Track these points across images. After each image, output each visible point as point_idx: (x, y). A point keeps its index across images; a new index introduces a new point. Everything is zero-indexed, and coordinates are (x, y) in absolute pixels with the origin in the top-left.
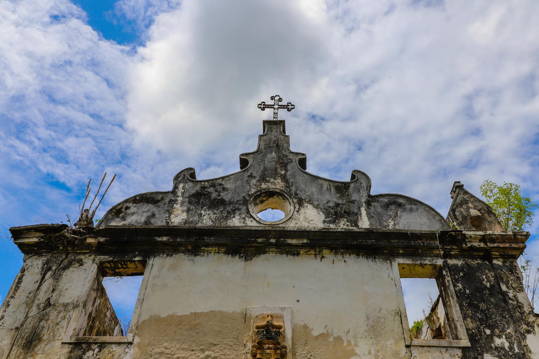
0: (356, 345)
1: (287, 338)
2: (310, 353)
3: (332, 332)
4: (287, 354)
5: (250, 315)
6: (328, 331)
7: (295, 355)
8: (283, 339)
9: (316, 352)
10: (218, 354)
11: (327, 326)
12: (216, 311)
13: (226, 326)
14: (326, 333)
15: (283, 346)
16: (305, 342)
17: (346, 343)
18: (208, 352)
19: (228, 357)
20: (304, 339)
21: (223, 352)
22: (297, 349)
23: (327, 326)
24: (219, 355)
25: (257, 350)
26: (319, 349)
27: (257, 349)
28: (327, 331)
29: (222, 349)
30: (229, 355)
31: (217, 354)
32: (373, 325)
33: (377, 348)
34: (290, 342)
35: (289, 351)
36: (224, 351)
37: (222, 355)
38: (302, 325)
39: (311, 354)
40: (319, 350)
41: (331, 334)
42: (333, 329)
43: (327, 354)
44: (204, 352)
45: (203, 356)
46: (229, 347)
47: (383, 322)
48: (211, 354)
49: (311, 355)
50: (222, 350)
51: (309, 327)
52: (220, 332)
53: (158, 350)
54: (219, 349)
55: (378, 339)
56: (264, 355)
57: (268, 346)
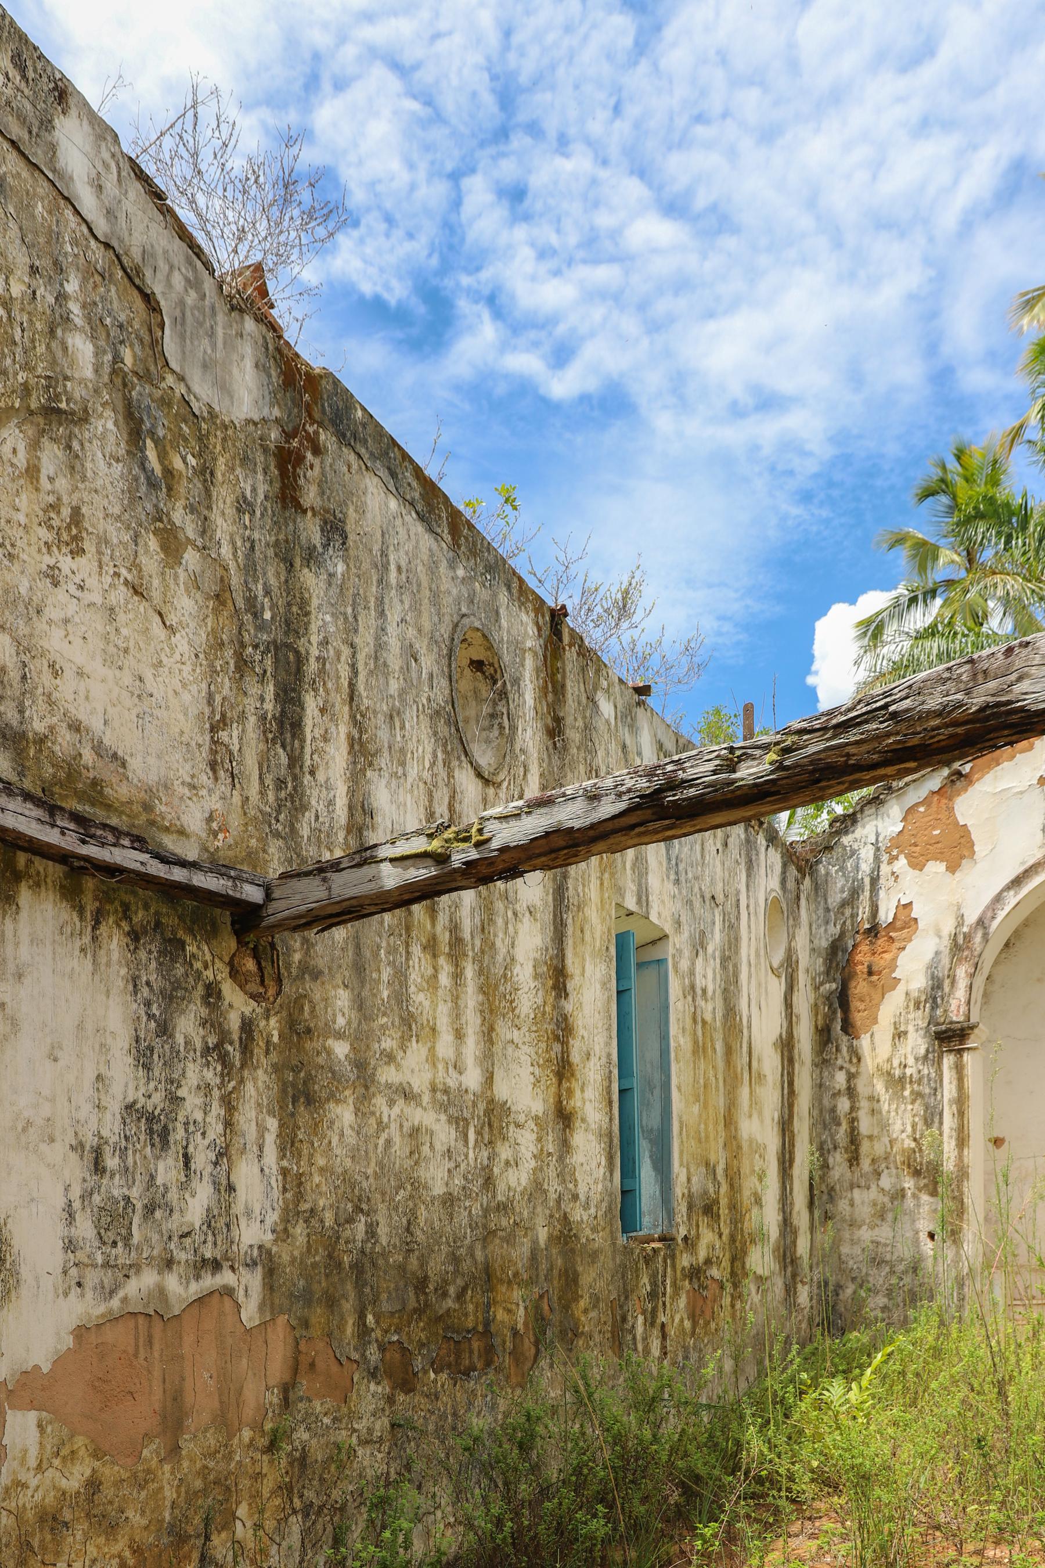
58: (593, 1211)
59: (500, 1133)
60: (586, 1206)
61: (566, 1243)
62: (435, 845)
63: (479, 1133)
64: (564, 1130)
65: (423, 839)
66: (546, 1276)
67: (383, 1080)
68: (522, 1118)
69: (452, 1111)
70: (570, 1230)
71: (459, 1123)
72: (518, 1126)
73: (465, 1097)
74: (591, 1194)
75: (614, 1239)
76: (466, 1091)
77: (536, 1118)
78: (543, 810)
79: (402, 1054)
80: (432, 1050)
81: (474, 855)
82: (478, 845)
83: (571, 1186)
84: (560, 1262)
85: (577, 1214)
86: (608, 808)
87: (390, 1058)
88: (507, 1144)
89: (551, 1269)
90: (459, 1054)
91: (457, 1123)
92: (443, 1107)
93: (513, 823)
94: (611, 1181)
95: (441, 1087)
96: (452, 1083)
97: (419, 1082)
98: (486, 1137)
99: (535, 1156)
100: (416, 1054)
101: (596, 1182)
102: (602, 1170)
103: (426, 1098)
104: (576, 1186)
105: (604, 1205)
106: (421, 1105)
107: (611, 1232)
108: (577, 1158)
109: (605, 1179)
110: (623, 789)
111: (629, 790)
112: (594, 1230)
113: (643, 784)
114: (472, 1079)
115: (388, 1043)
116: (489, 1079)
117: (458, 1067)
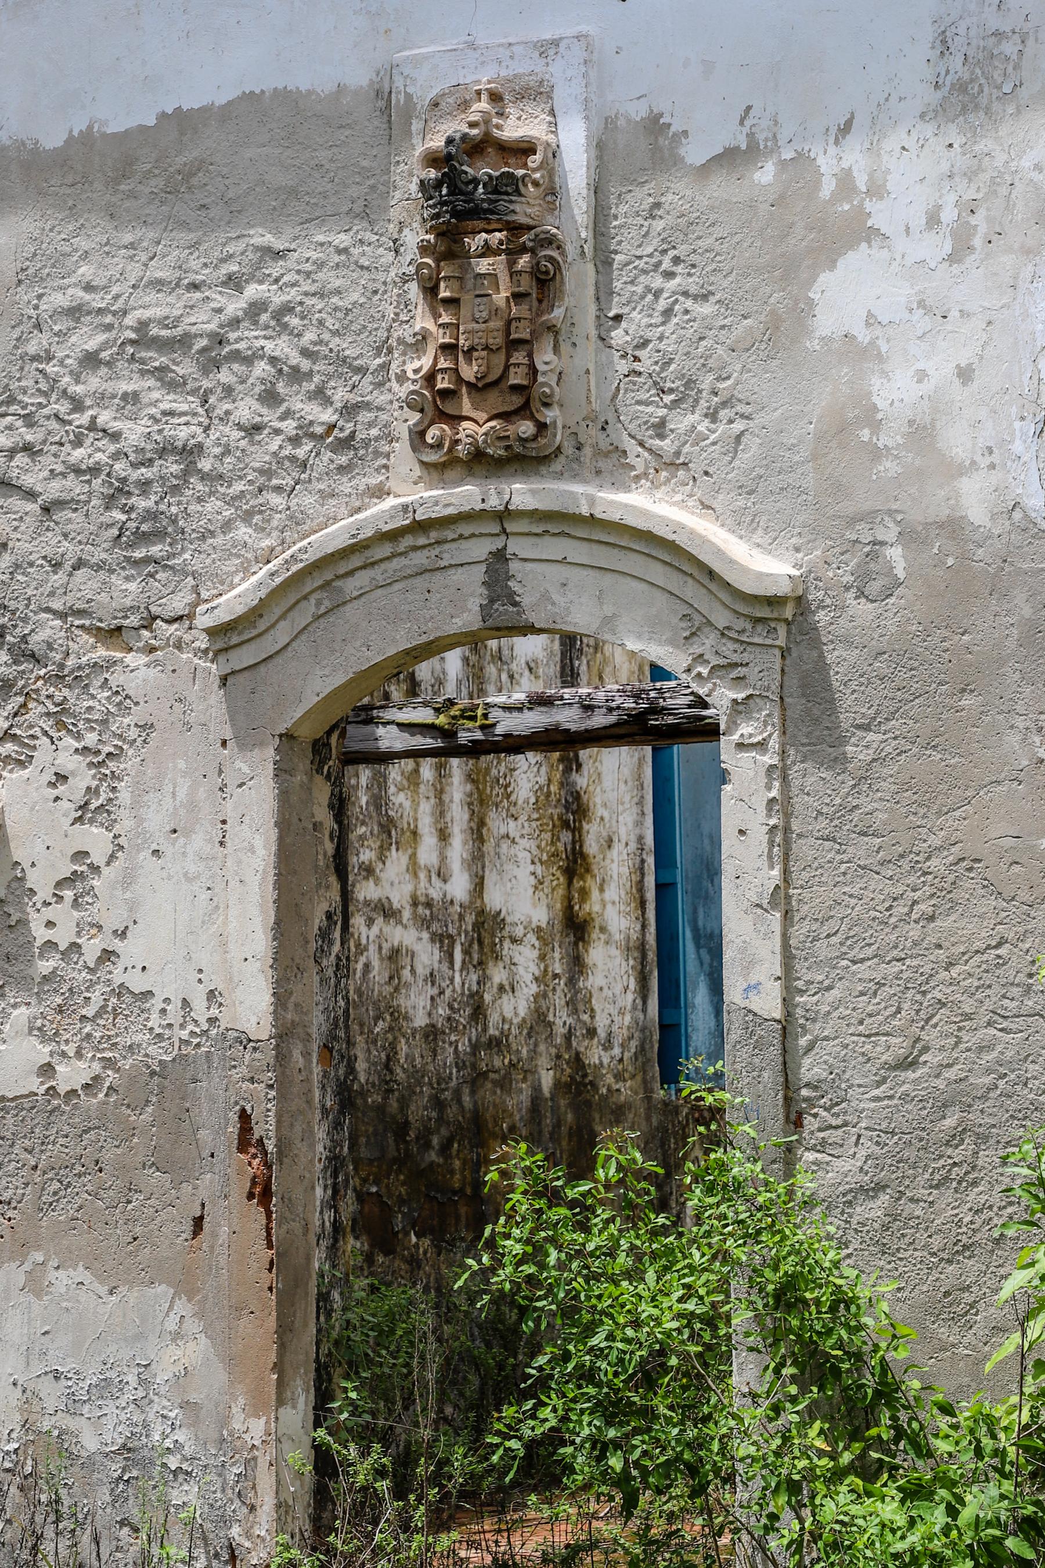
0: (877, 190)
1: (567, 190)
2: (674, 247)
3: (775, 136)
4: (560, 269)
5: (409, 97)
6: (753, 134)
7: (609, 263)
8: (549, 198)
9: (700, 243)
10: (293, 291)
11: (749, 108)
12: (263, 92)
13: (313, 163)
14: (744, 147)
15: (542, 236)
16: (651, 200)
17: (833, 187)
18: (256, 286)
19: (335, 300)
20: (647, 186)
21: (314, 281)
22: (618, 238)
23: (749, 108)
24: (298, 299)
25: (442, 264)
26: (713, 224)
27: (438, 261)
28: (751, 136)
29: (308, 267)
30: (338, 292)
31: (292, 295)
32: (966, 76)
33: (971, 194)
34: (580, 208)
35: (579, 251)
36: (320, 276)
37: (314, 295)
38: (638, 119)
39: (675, 252)
40: (711, 229)
41: (766, 147)
42: (776, 123)
43: (745, 245)
44: (239, 289)
45: (239, 306)
46: (337, 259)
47: (1015, 57)
48: (267, 294)
49: (676, 260)
50: (308, 274)
51: (670, 125)
52: (293, 192)
53: (59, 300)
54: (298, 272)
55: (980, 147)
56: (470, 283)
57: (486, 241)
58: (617, 1051)
59: (493, 951)
60: (607, 1045)
61: (579, 1093)
62: (442, 720)
63: (466, 952)
64: (576, 944)
65: (430, 711)
66: (551, 1134)
67: (361, 898)
68: (519, 931)
69: (435, 927)
70: (585, 1075)
71: (444, 941)
72: (514, 941)
73: (451, 910)
74: (615, 1028)
75: (648, 1090)
76: (452, 902)
77: (539, 929)
78: (543, 709)
79: (381, 865)
80: (413, 857)
81: (479, 735)
82: (483, 727)
83: (585, 1017)
84: (570, 1117)
85: (595, 1055)
86: (600, 720)
87: (369, 871)
88: (501, 964)
89: (558, 1125)
90: (443, 858)
91: (441, 942)
92: (424, 923)
93: (515, 714)
94: (644, 1010)
95: (422, 899)
96: (435, 894)
97: (399, 896)
98: (476, 956)
99: (536, 979)
100: (397, 862)
101: (621, 1012)
102: (630, 996)
103: (407, 914)
104: (592, 1017)
105: (634, 1044)
106: (401, 922)
107: (645, 1082)
108: (594, 981)
109: (634, 1008)
110: (614, 704)
111: (618, 708)
112: (619, 1077)
113: (630, 704)
114: (459, 887)
115: (367, 855)
116: (479, 886)
117: (443, 875)
